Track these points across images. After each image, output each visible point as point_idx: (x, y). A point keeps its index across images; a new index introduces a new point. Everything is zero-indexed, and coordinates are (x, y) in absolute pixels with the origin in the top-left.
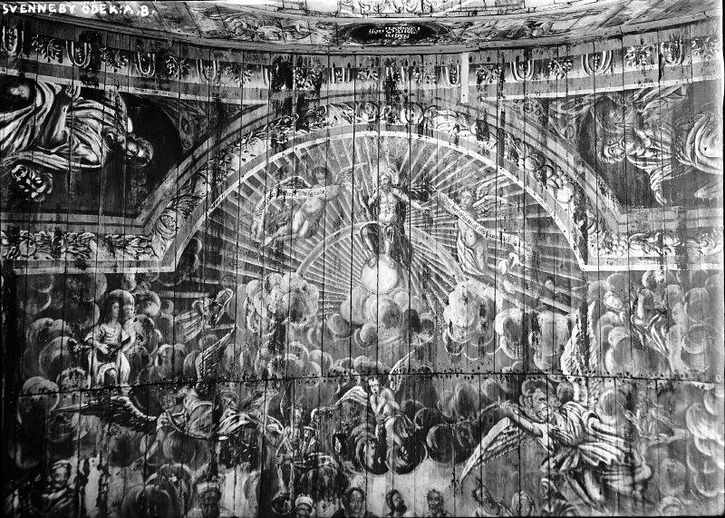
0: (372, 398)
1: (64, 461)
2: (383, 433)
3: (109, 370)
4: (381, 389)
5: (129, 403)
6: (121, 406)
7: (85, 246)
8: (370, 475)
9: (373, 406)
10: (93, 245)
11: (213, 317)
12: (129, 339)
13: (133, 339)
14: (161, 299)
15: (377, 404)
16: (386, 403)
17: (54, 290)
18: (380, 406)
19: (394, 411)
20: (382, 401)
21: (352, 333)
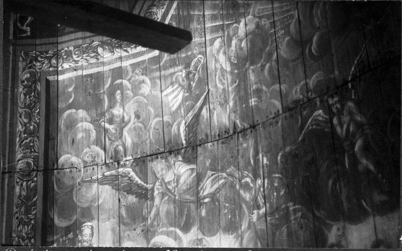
0: (335, 121)
1: (89, 224)
2: (355, 162)
3: (117, 146)
4: (343, 106)
5: (132, 174)
6: (127, 176)
7: (94, 52)
8: (348, 226)
9: (338, 129)
10: (100, 50)
11: (190, 85)
12: (130, 121)
13: (133, 117)
14: (150, 79)
15: (342, 127)
16: (352, 119)
17: (75, 88)
18: (345, 127)
19: (359, 126)
20: (346, 119)
21: (303, 53)
